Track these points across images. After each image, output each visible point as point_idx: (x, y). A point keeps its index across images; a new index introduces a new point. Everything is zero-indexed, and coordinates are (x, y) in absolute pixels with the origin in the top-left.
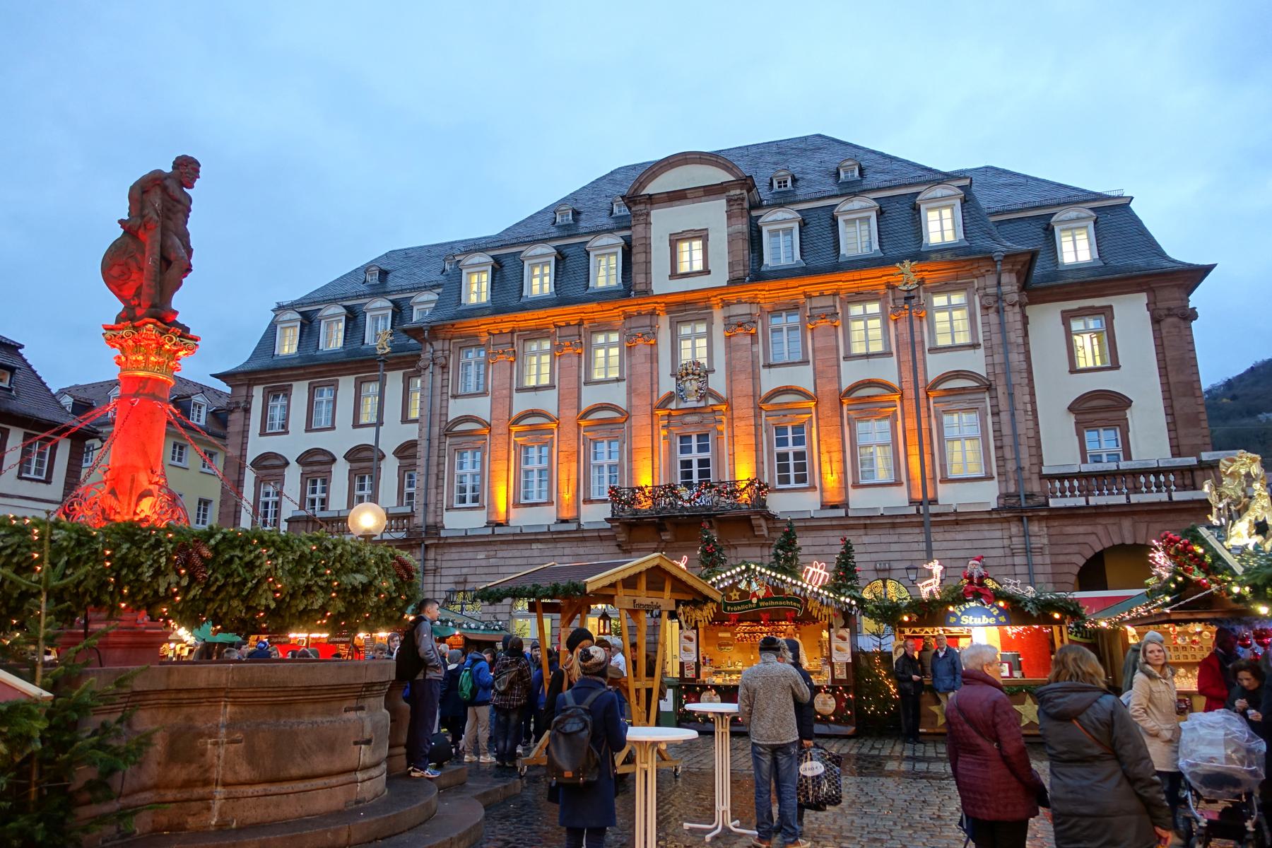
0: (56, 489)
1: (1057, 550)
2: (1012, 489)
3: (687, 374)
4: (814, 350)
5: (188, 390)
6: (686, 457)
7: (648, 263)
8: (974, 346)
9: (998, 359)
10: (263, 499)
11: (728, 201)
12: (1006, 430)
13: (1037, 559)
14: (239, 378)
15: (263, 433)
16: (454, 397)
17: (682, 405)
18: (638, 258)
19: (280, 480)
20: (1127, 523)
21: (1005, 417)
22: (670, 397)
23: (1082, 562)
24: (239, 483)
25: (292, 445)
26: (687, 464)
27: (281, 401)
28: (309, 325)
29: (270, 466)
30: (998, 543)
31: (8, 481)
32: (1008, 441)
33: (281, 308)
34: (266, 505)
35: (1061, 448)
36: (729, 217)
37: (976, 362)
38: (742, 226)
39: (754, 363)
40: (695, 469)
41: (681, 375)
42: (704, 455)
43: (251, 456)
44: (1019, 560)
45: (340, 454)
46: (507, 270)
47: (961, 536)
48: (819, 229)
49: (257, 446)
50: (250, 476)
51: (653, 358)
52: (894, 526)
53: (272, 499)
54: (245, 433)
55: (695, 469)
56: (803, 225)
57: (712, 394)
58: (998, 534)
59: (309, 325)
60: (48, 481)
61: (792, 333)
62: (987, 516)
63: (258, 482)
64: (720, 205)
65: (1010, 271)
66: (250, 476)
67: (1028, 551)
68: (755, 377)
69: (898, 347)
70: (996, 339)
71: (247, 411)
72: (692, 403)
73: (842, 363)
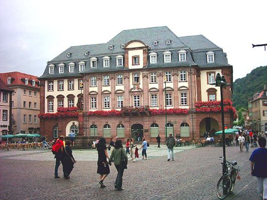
0: (8, 104)
2: (191, 108)
5: (23, 77)
7: (128, 62)
8: (187, 81)
12: (191, 97)
14: (42, 80)
15: (48, 91)
18: (126, 61)
19: (53, 101)
21: (190, 95)
22: (132, 89)
26: (135, 101)
27: (51, 84)
28: (56, 67)
29: (51, 98)
31: (2, 103)
35: (205, 98)
36: (143, 53)
37: (186, 84)
38: (146, 56)
39: (148, 83)
40: (137, 102)
41: (134, 85)
45: (65, 96)
46: (100, 61)
48: (160, 56)
49: (47, 94)
50: (46, 100)
51: (129, 81)
53: (51, 105)
55: (137, 102)
56: (158, 55)
57: (140, 89)
59: (56, 67)
60: (7, 102)
61: (167, 57)
63: (48, 101)
66: (46, 100)
68: (148, 86)
70: (190, 80)
71: (44, 86)
72: (136, 90)
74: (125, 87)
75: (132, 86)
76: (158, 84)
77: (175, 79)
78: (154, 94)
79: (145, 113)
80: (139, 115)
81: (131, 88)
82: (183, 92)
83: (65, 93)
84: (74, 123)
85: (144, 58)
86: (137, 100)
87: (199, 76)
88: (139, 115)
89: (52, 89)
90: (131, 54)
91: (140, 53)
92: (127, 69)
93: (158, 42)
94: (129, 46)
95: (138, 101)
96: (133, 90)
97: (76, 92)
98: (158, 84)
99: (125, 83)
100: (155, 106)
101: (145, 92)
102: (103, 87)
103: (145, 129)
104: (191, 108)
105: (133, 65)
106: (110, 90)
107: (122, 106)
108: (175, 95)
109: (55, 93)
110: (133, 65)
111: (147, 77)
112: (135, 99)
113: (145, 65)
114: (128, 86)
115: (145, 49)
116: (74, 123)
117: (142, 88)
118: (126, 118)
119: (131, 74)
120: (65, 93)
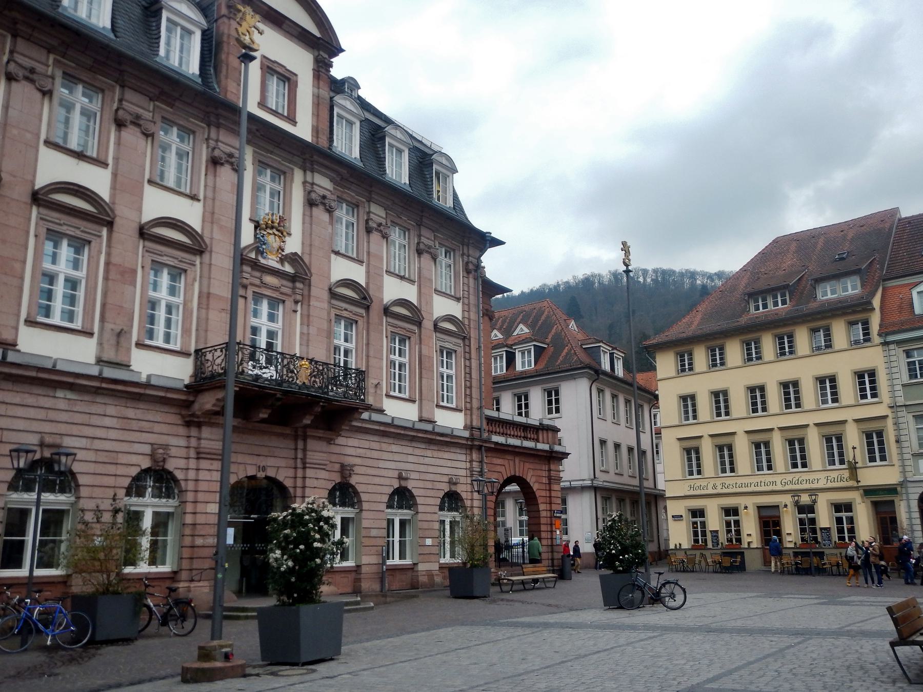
3: (272, 228)
30: (463, 465)
47: (446, 455)
52: (413, 439)
58: (463, 457)
62: (464, 442)
69: (420, 277)
74: (209, 217)
102: (46, 156)
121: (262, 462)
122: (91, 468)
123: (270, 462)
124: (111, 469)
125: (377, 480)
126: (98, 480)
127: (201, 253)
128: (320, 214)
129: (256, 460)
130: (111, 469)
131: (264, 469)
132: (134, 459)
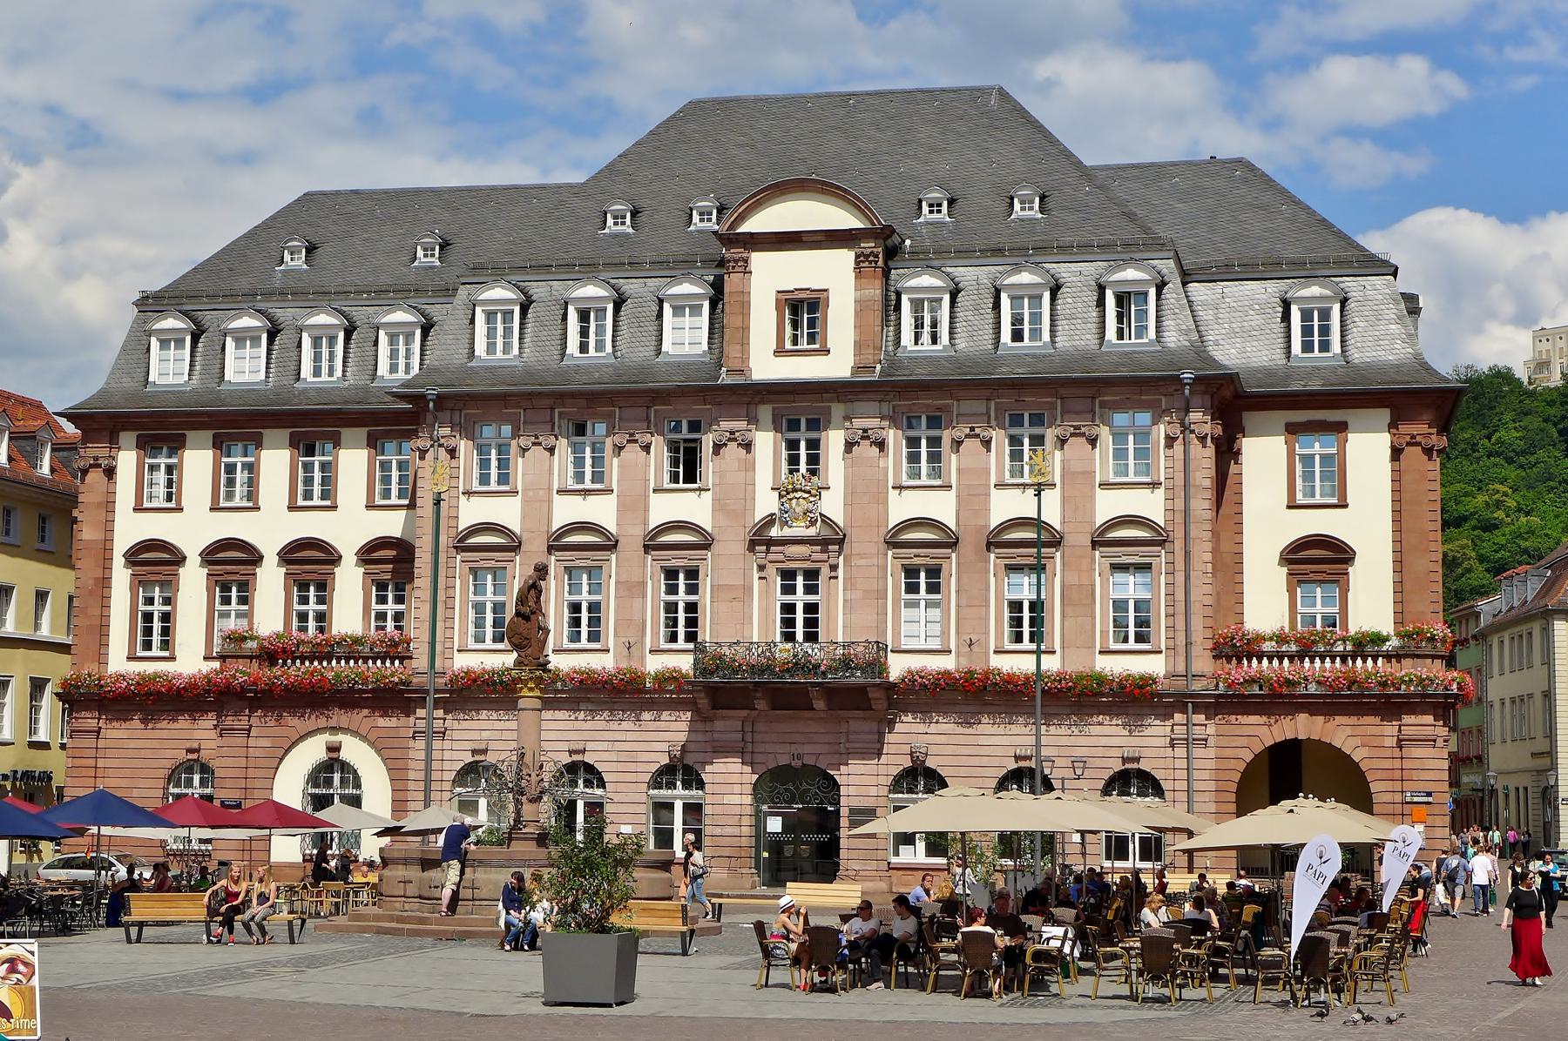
1: (1224, 742)
2: (1181, 669)
3: (794, 490)
4: (959, 470)
6: (788, 598)
7: (745, 329)
8: (1154, 485)
9: (1179, 504)
10: (142, 607)
11: (857, 256)
12: (1180, 595)
13: (1198, 752)
15: (139, 508)
16: (468, 493)
17: (787, 532)
18: (731, 320)
19: (170, 585)
20: (1302, 718)
21: (1180, 577)
22: (770, 521)
23: (1249, 757)
24: (105, 582)
25: (192, 530)
26: (789, 608)
29: (156, 561)
32: (1181, 607)
33: (151, 304)
34: (148, 617)
37: (1152, 506)
38: (875, 291)
40: (800, 616)
41: (784, 492)
42: (812, 598)
43: (123, 541)
44: (1181, 752)
49: (130, 529)
50: (121, 576)
51: (750, 467)
54: (109, 505)
55: (800, 616)
57: (826, 521)
63: (138, 582)
64: (844, 259)
65: (1204, 393)
67: (1189, 742)
69: (1063, 476)
72: (799, 530)
73: (993, 489)
74: (718, 507)
75: (766, 503)
76: (951, 495)
77: (1076, 466)
78: (923, 559)
79: (862, 699)
80: (819, 704)
81: (760, 514)
82: (1127, 545)
83: (271, 528)
84: (334, 749)
85: (861, 307)
86: (682, 597)
87: (1227, 453)
88: (819, 704)
89: (169, 498)
90: (770, 276)
91: (834, 273)
92: (739, 380)
93: (951, 202)
94: (763, 221)
95: (811, 608)
96: (774, 532)
97: (352, 524)
98: (951, 495)
99: (719, 474)
100: (919, 642)
101: (864, 544)
103: (855, 803)
104: (1181, 669)
105: (780, 352)
106: (610, 524)
107: (691, 637)
108: (1073, 578)
109: (192, 530)
110: (780, 352)
111: (881, 445)
112: (789, 589)
113: (868, 358)
114: (732, 502)
115: (868, 245)
116: (334, 749)
117: (838, 517)
118: (719, 725)
119: (765, 412)
120: (271, 528)
121: (796, 749)
122: (614, 767)
123: (808, 749)
124: (632, 767)
125: (985, 761)
126: (621, 777)
127: (707, 547)
128: (867, 450)
129: (787, 748)
130: (632, 767)
131: (799, 757)
132: (653, 757)
